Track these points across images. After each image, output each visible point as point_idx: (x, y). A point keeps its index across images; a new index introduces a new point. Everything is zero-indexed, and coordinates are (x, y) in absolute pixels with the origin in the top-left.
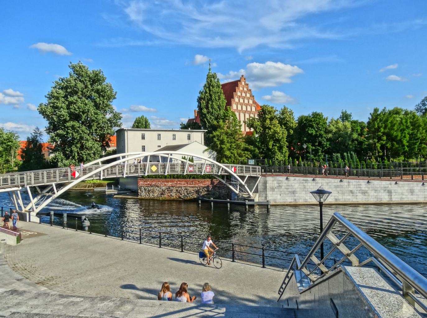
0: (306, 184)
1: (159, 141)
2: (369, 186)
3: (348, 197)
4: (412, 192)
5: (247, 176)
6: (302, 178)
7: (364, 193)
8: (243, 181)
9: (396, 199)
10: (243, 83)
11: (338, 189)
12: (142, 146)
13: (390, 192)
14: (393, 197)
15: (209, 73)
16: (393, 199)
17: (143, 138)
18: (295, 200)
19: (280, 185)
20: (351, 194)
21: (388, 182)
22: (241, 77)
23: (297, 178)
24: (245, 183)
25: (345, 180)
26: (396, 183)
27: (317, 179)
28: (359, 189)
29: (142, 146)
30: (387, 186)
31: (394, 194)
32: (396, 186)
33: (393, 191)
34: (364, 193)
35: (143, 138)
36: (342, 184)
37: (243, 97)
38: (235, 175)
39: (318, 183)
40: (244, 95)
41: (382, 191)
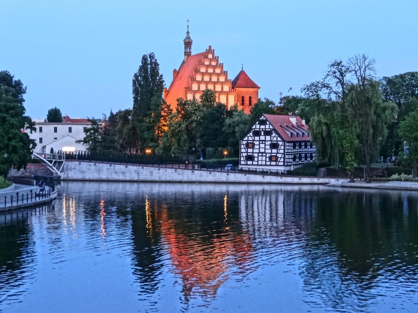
0: (90, 167)
1: (56, 134)
2: (126, 169)
3: (114, 176)
4: (151, 173)
5: (54, 160)
6: (88, 163)
7: (123, 173)
8: (51, 163)
9: (142, 178)
10: (210, 56)
11: (109, 171)
12: (40, 138)
13: (138, 174)
14: (140, 177)
15: (186, 38)
16: (140, 179)
17: (56, 130)
18: (84, 177)
19: (76, 167)
20: (116, 174)
21: (138, 167)
22: (208, 48)
23: (85, 163)
24: (53, 165)
25: (112, 165)
26: (143, 168)
27: (96, 164)
28: (121, 171)
29: (40, 138)
30: (136, 169)
31: (141, 175)
32: (142, 170)
33: (140, 173)
34: (123, 173)
35: (56, 130)
36: (111, 167)
37: (209, 73)
38: (45, 160)
39: (97, 166)
40: (210, 70)
41: (134, 173)
